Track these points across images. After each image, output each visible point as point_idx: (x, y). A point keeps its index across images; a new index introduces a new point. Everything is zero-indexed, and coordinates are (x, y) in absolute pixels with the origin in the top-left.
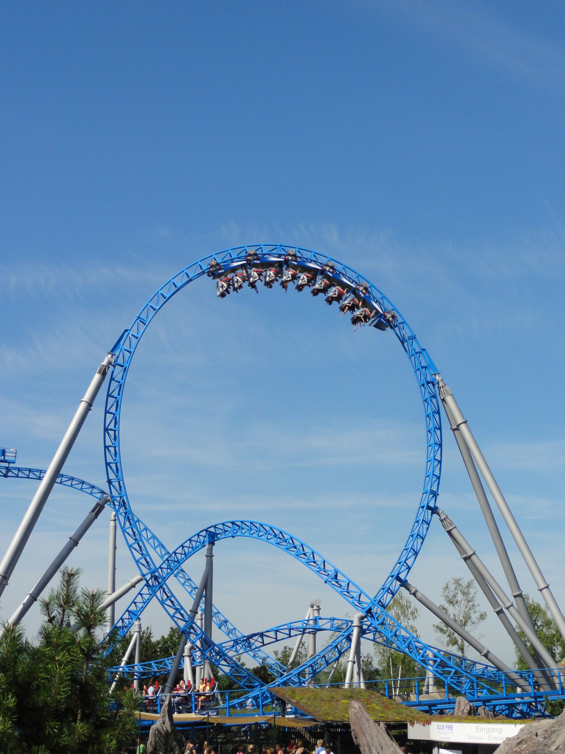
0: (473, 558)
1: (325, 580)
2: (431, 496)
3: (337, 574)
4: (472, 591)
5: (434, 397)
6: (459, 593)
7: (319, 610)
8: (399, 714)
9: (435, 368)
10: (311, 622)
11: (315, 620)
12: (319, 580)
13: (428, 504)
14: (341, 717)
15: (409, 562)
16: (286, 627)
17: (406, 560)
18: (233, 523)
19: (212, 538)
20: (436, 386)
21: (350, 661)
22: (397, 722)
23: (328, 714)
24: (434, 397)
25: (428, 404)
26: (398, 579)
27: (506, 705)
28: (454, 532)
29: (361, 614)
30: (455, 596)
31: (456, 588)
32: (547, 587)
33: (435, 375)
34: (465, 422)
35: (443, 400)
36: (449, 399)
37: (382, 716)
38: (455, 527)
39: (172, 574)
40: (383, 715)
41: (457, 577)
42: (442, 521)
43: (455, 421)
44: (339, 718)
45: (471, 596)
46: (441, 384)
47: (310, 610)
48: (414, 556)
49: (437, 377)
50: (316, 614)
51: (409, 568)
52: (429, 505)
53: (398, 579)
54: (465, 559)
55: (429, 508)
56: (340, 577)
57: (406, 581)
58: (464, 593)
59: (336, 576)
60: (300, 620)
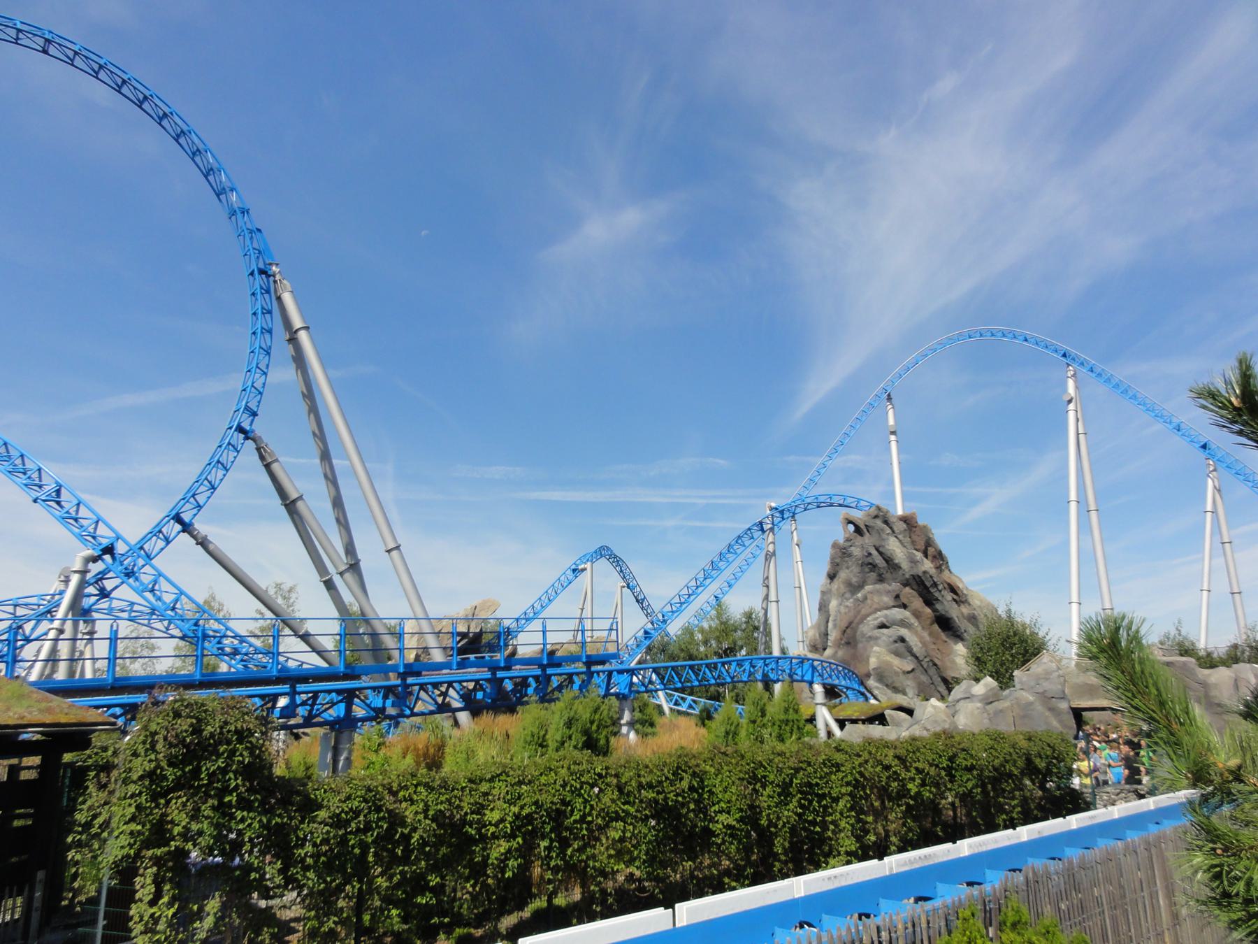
0: (300, 504)
1: (35, 497)
2: (245, 416)
4: (293, 595)
5: (268, 292)
6: (279, 597)
12: (25, 498)
15: (201, 499)
20: (271, 279)
21: (53, 629)
24: (268, 292)
25: (256, 299)
26: (178, 519)
27: (339, 692)
28: (275, 467)
29: (89, 552)
31: (276, 593)
32: (397, 548)
33: (271, 264)
34: (307, 328)
35: (279, 299)
36: (287, 298)
38: (277, 460)
41: (279, 582)
45: (291, 601)
46: (278, 277)
47: (57, 583)
48: (208, 493)
49: (274, 268)
51: (199, 507)
52: (242, 424)
53: (178, 519)
54: (286, 506)
55: (240, 429)
56: (65, 495)
57: (191, 524)
58: (284, 598)
59: (58, 492)
60: (35, 594)
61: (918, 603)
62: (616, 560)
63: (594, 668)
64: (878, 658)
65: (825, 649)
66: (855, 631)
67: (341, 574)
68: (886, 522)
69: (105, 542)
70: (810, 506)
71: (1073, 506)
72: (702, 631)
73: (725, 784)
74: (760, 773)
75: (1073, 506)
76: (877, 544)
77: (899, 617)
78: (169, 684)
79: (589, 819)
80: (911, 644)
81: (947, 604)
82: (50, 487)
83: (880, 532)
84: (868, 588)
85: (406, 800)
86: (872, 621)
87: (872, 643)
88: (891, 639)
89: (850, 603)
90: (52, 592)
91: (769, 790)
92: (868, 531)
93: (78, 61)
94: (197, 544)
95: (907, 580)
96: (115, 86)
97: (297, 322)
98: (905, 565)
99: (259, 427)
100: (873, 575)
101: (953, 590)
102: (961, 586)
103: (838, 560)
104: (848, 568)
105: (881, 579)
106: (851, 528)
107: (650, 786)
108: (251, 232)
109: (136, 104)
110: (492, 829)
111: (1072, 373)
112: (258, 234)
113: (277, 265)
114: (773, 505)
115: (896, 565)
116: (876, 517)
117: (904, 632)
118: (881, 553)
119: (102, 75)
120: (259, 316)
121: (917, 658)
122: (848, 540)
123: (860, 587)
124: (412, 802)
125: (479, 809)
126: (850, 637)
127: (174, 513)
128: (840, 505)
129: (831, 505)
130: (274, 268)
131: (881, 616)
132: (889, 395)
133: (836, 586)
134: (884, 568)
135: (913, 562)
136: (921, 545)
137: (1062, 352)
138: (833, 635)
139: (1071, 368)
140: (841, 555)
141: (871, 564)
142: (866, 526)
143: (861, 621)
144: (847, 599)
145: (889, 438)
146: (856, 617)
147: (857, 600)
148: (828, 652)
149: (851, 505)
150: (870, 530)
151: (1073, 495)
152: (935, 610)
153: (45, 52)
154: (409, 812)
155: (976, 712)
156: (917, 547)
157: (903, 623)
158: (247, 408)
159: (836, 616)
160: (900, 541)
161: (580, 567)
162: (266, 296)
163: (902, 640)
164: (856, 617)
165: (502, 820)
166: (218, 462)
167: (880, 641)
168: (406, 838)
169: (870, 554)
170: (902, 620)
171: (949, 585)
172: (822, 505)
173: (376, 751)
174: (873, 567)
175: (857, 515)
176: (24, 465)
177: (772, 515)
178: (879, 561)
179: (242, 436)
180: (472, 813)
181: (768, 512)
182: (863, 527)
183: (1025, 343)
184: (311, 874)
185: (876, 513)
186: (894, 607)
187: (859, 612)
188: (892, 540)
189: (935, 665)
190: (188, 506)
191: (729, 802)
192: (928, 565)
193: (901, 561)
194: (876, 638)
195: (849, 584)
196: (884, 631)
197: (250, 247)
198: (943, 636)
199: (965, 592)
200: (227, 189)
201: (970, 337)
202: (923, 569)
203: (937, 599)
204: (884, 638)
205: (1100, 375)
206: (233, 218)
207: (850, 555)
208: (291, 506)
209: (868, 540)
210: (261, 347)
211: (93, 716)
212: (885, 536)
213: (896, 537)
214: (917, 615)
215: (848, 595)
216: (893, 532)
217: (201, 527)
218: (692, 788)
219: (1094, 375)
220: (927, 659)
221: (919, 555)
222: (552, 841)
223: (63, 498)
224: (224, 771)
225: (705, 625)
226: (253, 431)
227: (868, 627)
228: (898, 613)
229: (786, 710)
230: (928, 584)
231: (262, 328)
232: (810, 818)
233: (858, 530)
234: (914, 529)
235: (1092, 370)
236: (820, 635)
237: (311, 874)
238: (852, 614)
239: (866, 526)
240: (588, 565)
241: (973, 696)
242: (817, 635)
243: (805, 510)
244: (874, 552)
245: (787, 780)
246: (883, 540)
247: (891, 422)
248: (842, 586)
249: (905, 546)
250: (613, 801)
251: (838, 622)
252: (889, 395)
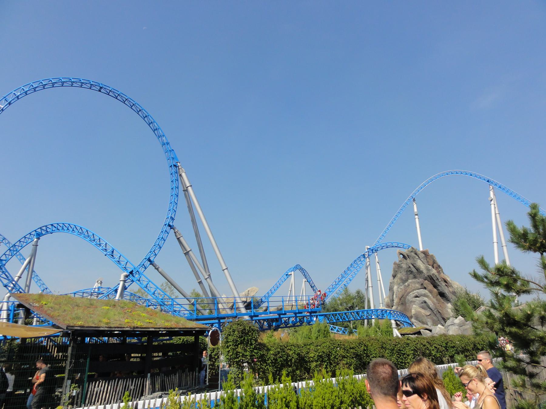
0: (190, 252)
3: (113, 251)
5: (177, 173)
7: (101, 283)
8: (168, 321)
9: (177, 160)
10: (96, 290)
11: (99, 288)
13: (169, 223)
14: (96, 322)
16: (81, 291)
17: (155, 250)
18: (52, 225)
19: (39, 236)
20: (178, 168)
22: (167, 328)
23: (78, 318)
24: (177, 173)
26: (149, 260)
28: (181, 239)
29: (126, 273)
30: (165, 289)
32: (227, 269)
33: (177, 163)
34: (191, 186)
35: (181, 175)
36: (184, 175)
37: (150, 322)
38: (182, 236)
39: (26, 270)
40: (151, 321)
42: (175, 233)
43: (186, 185)
44: (93, 323)
45: (172, 289)
46: (180, 167)
47: (96, 284)
48: (159, 249)
49: (178, 164)
50: (99, 285)
51: (156, 255)
53: (149, 260)
55: (169, 226)
59: (113, 252)
61: (431, 287)
62: (302, 270)
63: (312, 314)
64: (415, 310)
65: (393, 306)
66: (405, 298)
67: (206, 279)
68: (416, 254)
69: (130, 270)
70: (384, 248)
71: (495, 245)
72: (339, 300)
73: (374, 349)
74: (384, 346)
75: (495, 245)
76: (413, 263)
77: (423, 293)
78: (230, 317)
79: (337, 357)
80: (429, 304)
81: (443, 287)
82: (109, 250)
83: (413, 258)
84: (410, 281)
85: (289, 350)
86: (412, 295)
87: (412, 303)
88: (420, 302)
89: (402, 287)
90: (94, 287)
91: (387, 351)
92: (408, 257)
93: (126, 102)
94: (155, 269)
95: (426, 277)
96: (130, 106)
97: (188, 184)
98: (425, 271)
99: (175, 224)
100: (411, 276)
101: (445, 281)
102: (448, 280)
103: (396, 270)
104: (401, 273)
105: (415, 277)
106: (401, 256)
107: (353, 348)
108: (170, 151)
109: (122, 102)
110: (312, 359)
111: (491, 188)
112: (173, 151)
113: (179, 162)
114: (369, 247)
115: (421, 271)
116: (412, 252)
117: (426, 299)
118: (414, 267)
119: (133, 107)
120: (174, 182)
121: (431, 309)
122: (400, 261)
123: (406, 280)
124: (291, 350)
125: (308, 353)
126: (403, 301)
127: (148, 257)
128: (396, 247)
129: (393, 247)
130: (178, 164)
131: (416, 292)
132: (414, 199)
133: (396, 280)
134: (416, 273)
135: (428, 270)
136: (431, 263)
137: (487, 180)
138: (396, 301)
139: (491, 186)
140: (398, 267)
141: (410, 271)
142: (408, 255)
143: (407, 295)
144: (401, 286)
145: (415, 217)
146: (405, 293)
147: (405, 286)
148: (394, 308)
151: (495, 240)
152: (438, 290)
153: (100, 91)
154: (291, 353)
155: (456, 330)
156: (429, 264)
157: (425, 295)
158: (171, 217)
159: (397, 293)
160: (422, 261)
161: (289, 274)
162: (176, 174)
163: (425, 302)
164: (405, 293)
165: (314, 356)
166: (162, 238)
167: (416, 303)
168: (291, 360)
169: (410, 267)
170: (425, 294)
171: (443, 279)
172: (389, 247)
173: (271, 338)
174: (411, 272)
175: (405, 251)
176: (100, 242)
177: (368, 252)
178: (413, 269)
179: (169, 227)
180: (306, 354)
181: (367, 250)
182: (406, 256)
183: (471, 176)
184: (271, 368)
185: (411, 250)
186: (421, 289)
187: (406, 291)
188: (419, 261)
189: (439, 312)
190: (152, 255)
191: (376, 354)
192: (434, 271)
193: (423, 269)
194: (414, 302)
195: (401, 279)
196: (417, 298)
197: (170, 157)
198: (442, 300)
199: (450, 282)
200: (162, 136)
201: (447, 174)
202: (432, 273)
203: (439, 285)
204: (417, 301)
205: (504, 189)
206: (164, 146)
207: (401, 267)
208: (187, 254)
209: (408, 261)
210: (175, 194)
211: (207, 326)
212: (415, 259)
214: (431, 292)
215: (401, 284)
216: (419, 258)
217: (156, 261)
218: (364, 350)
219: (501, 189)
220: (436, 310)
221: (430, 267)
222: (327, 363)
223: (114, 254)
224: (251, 340)
225: (341, 297)
226: (173, 226)
227: (410, 297)
228: (423, 291)
229: (387, 328)
230: (435, 279)
231: (176, 187)
232: (401, 361)
233: (404, 257)
234: (428, 256)
236: (390, 300)
237: (271, 368)
238: (403, 291)
239: (408, 255)
240: (293, 273)
241: (455, 323)
242: (389, 300)
243: (382, 249)
244: (412, 266)
245: (393, 348)
246: (415, 261)
247: (416, 210)
248: (399, 280)
249: (424, 264)
250: (343, 352)
251: (398, 295)
252: (414, 199)
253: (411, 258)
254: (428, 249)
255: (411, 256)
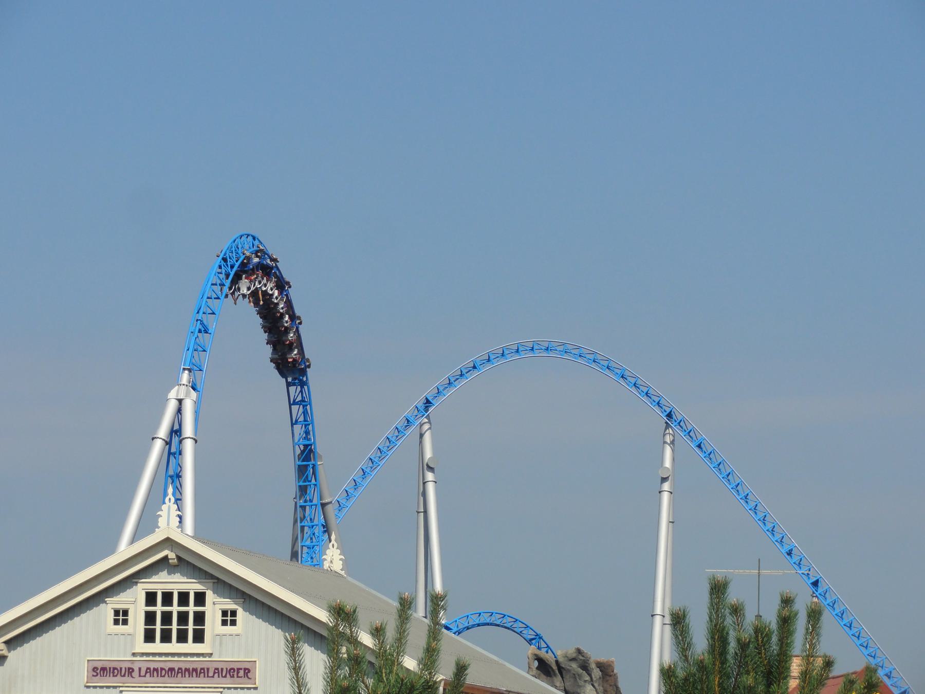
83: (575, 677)
116: (573, 659)
132: (426, 409)
137: (668, 410)
142: (560, 669)
149: (515, 629)
150: (564, 673)
182: (555, 667)
185: (574, 655)
212: (581, 683)
213: (593, 685)
234: (608, 678)
235: (699, 446)
246: (580, 687)
253: (567, 677)
254: (613, 659)
255: (569, 671)
